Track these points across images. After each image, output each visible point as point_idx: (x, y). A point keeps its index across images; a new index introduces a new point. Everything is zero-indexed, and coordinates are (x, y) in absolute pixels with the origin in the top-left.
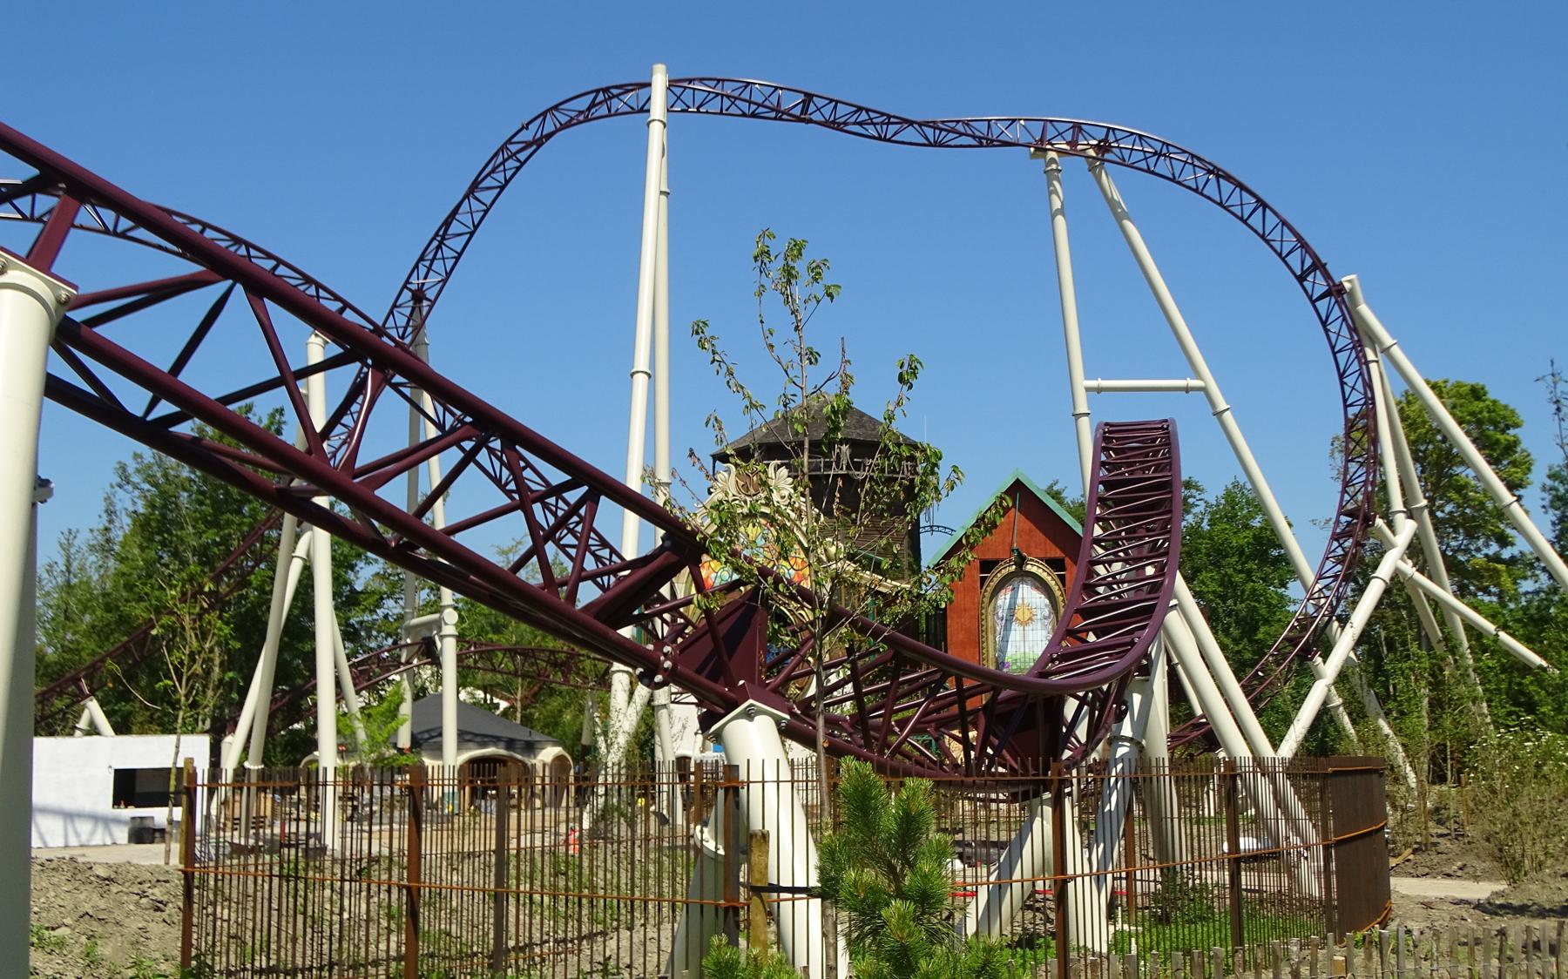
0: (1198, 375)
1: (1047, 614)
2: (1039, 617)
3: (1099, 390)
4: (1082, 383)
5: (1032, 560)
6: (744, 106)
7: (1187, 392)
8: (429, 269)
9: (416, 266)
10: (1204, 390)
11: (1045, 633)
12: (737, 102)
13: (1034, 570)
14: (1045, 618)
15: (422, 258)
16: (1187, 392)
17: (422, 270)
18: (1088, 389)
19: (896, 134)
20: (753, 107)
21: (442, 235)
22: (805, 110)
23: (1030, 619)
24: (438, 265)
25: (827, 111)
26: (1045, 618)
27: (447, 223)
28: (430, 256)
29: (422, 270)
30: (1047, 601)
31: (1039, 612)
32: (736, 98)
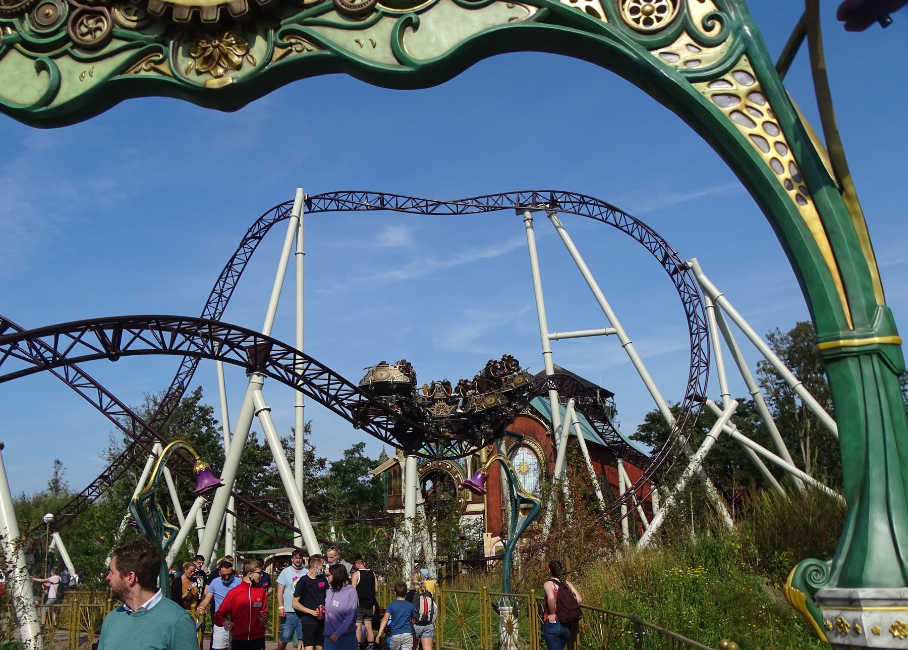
1: (536, 468)
2: (532, 469)
5: (527, 437)
6: (350, 205)
8: (225, 282)
9: (218, 281)
11: (535, 478)
12: (346, 204)
13: (528, 442)
14: (535, 470)
15: (220, 278)
17: (221, 283)
19: (433, 210)
20: (355, 205)
21: (229, 267)
22: (382, 202)
23: (527, 471)
24: (229, 280)
25: (393, 203)
26: (535, 470)
27: (232, 260)
28: (224, 276)
29: (221, 283)
30: (536, 460)
31: (532, 466)
32: (345, 202)
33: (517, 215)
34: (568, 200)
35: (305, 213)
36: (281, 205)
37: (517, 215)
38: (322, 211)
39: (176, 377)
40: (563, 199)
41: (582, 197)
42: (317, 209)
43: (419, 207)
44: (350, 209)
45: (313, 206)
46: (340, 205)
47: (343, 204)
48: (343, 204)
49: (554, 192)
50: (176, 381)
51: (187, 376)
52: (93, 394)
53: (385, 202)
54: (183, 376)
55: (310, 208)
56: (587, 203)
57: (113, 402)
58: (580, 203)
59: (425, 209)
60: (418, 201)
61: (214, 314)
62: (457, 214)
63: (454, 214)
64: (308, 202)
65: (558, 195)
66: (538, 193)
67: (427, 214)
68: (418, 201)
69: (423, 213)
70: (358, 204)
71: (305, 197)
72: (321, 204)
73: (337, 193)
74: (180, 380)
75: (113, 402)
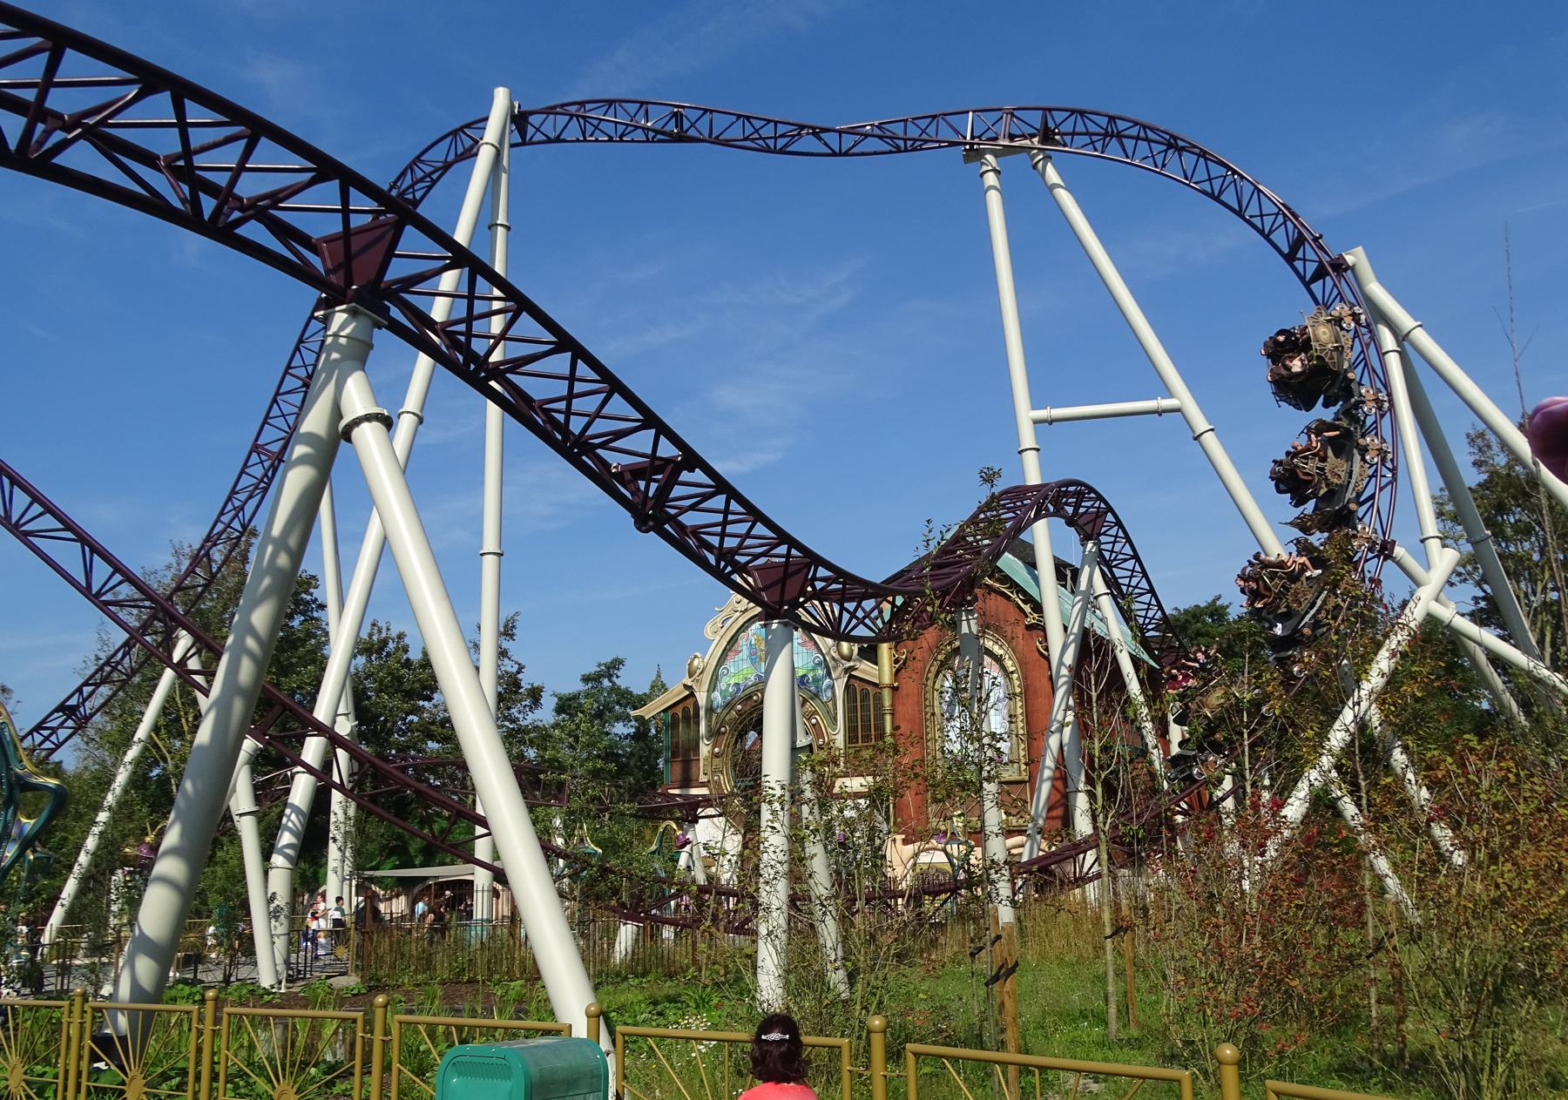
0: (1169, 394)
3: (1051, 421)
4: (1026, 414)
7: (1160, 415)
10: (1178, 410)
16: (1160, 415)
18: (1036, 422)
33: (966, 162)
34: (1080, 128)
35: (512, 146)
36: (461, 129)
37: (966, 162)
38: (549, 141)
39: (229, 499)
40: (1067, 127)
41: (1112, 119)
42: (539, 137)
43: (761, 138)
44: (611, 140)
45: (531, 131)
46: (590, 129)
47: (596, 127)
48: (596, 127)
49: (1050, 110)
50: (230, 507)
51: (250, 497)
52: (69, 555)
53: (686, 125)
54: (242, 496)
55: (523, 134)
56: (1119, 136)
57: (118, 577)
58: (1106, 135)
59: (771, 143)
60: (758, 124)
61: (315, 366)
62: (840, 154)
63: (834, 154)
64: (518, 120)
65: (1059, 116)
66: (1016, 113)
67: (775, 151)
68: (758, 124)
69: (768, 150)
70: (627, 125)
71: (512, 107)
72: (551, 126)
73: (582, 104)
74: (237, 504)
75: (118, 577)
